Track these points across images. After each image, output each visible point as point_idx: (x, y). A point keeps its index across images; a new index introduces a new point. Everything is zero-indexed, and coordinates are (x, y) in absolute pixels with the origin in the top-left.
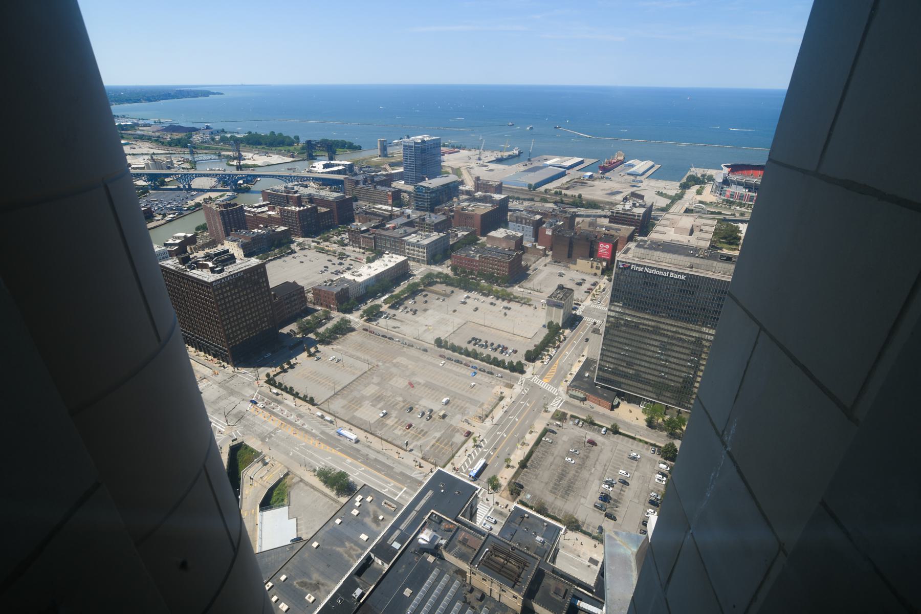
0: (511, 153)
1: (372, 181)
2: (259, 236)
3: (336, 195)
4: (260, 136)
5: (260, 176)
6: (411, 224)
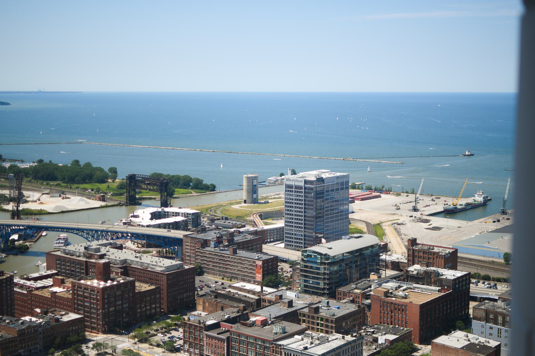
0: (470, 200)
1: (231, 241)
2: (33, 328)
3: (168, 263)
4: (57, 167)
5: (47, 228)
6: (293, 317)
